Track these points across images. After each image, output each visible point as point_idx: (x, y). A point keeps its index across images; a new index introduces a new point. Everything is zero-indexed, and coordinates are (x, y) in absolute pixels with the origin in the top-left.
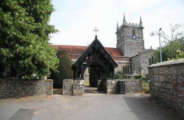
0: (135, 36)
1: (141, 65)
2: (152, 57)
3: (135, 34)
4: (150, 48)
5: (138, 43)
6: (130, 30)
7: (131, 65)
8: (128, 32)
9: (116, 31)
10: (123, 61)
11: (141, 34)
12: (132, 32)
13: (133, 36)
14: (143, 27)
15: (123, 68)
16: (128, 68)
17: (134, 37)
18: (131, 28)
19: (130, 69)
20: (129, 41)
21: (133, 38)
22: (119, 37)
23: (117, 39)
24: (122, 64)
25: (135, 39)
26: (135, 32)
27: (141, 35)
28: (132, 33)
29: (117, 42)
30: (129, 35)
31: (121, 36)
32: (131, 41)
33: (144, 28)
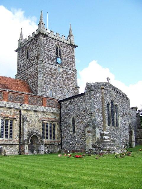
0: (61, 59)
1: (93, 118)
2: (112, 101)
3: (60, 55)
4: (106, 81)
5: (66, 73)
6: (53, 45)
7: (61, 118)
8: (47, 48)
9: (16, 46)
10: (43, 107)
11: (72, 58)
12: (55, 49)
13: (57, 58)
14: (75, 44)
15: (43, 123)
16: (54, 125)
17: (59, 60)
18: (54, 42)
19: (57, 127)
20: (49, 66)
21: (57, 63)
22: (25, 57)
23: (18, 62)
24: (40, 115)
25: (61, 64)
26: (60, 50)
27: (71, 60)
28: (55, 51)
29: (19, 69)
30: (49, 53)
31: (31, 56)
32: (54, 67)
33: (76, 47)
